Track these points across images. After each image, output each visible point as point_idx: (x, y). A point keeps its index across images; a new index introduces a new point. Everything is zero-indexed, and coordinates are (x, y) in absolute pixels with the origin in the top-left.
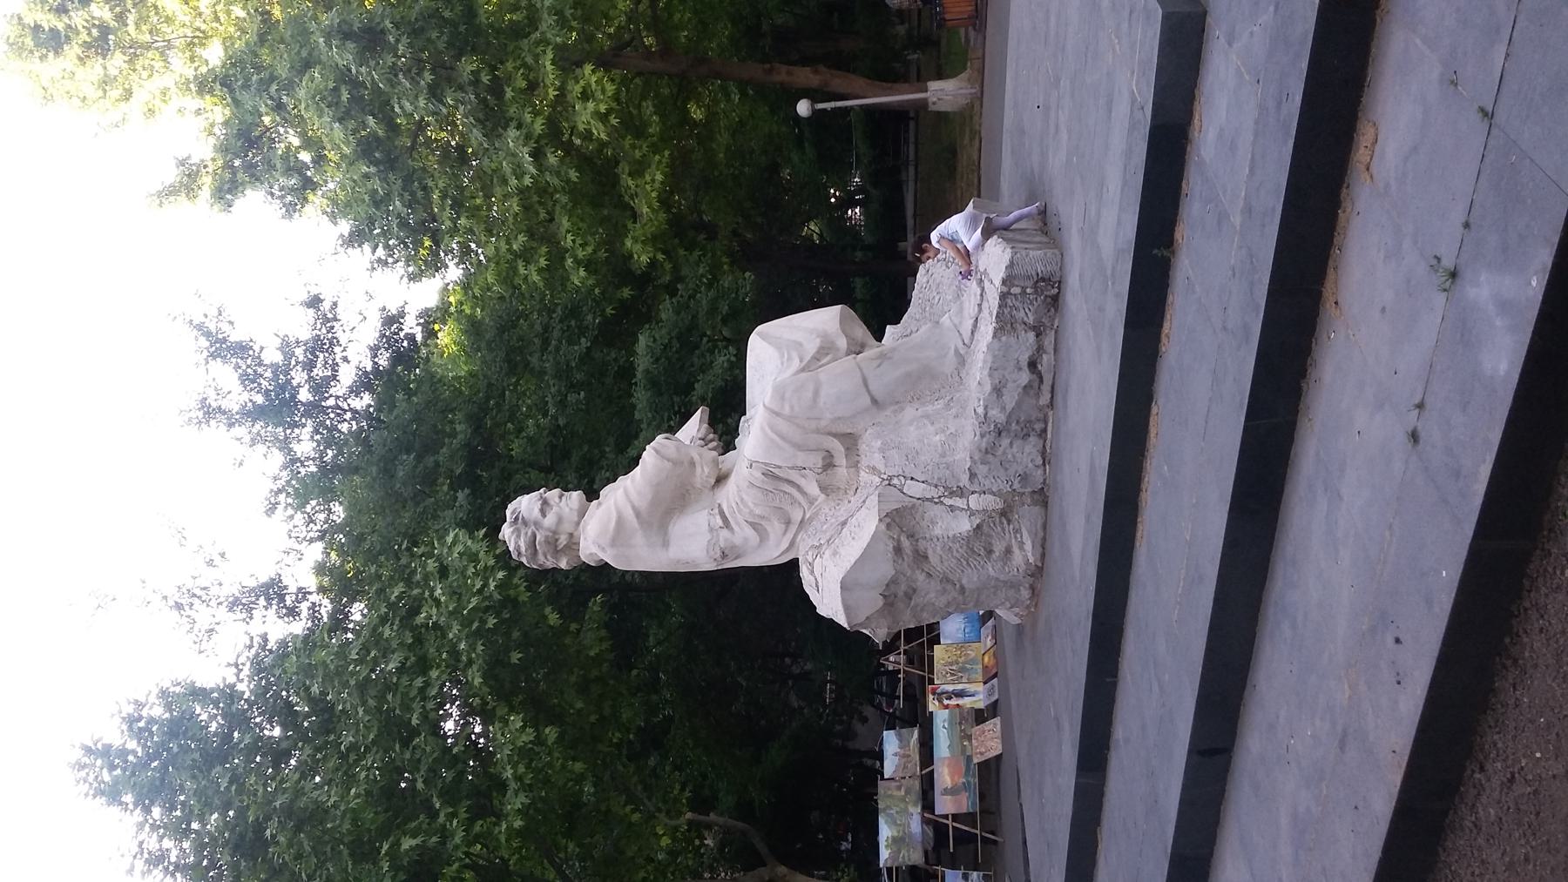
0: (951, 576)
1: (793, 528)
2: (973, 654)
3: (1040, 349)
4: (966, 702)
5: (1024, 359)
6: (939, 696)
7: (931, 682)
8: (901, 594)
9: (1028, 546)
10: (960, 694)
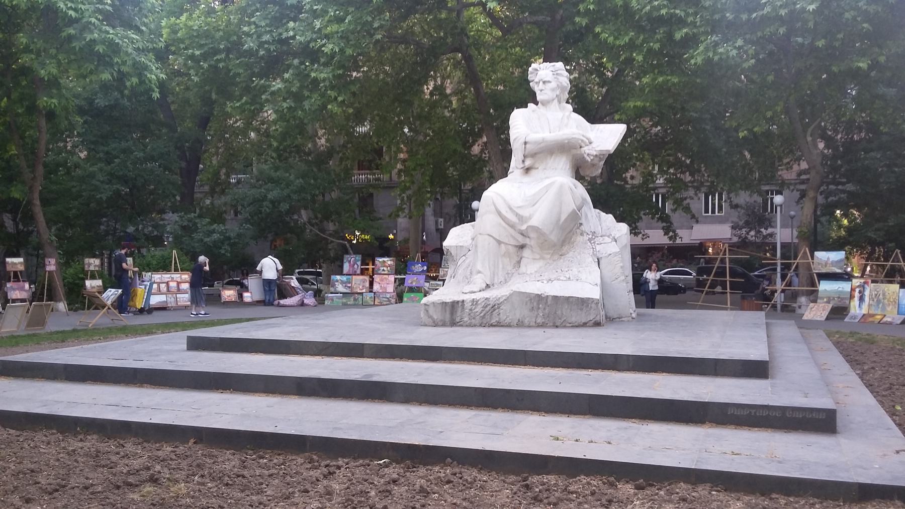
2: (889, 309)
4: (855, 302)
6: (862, 287)
7: (873, 282)
10: (861, 299)
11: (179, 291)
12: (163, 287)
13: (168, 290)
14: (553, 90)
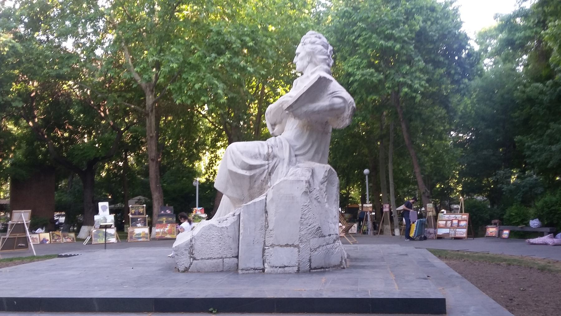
11: (458, 226)
12: (449, 223)
13: (451, 226)
14: (302, 59)
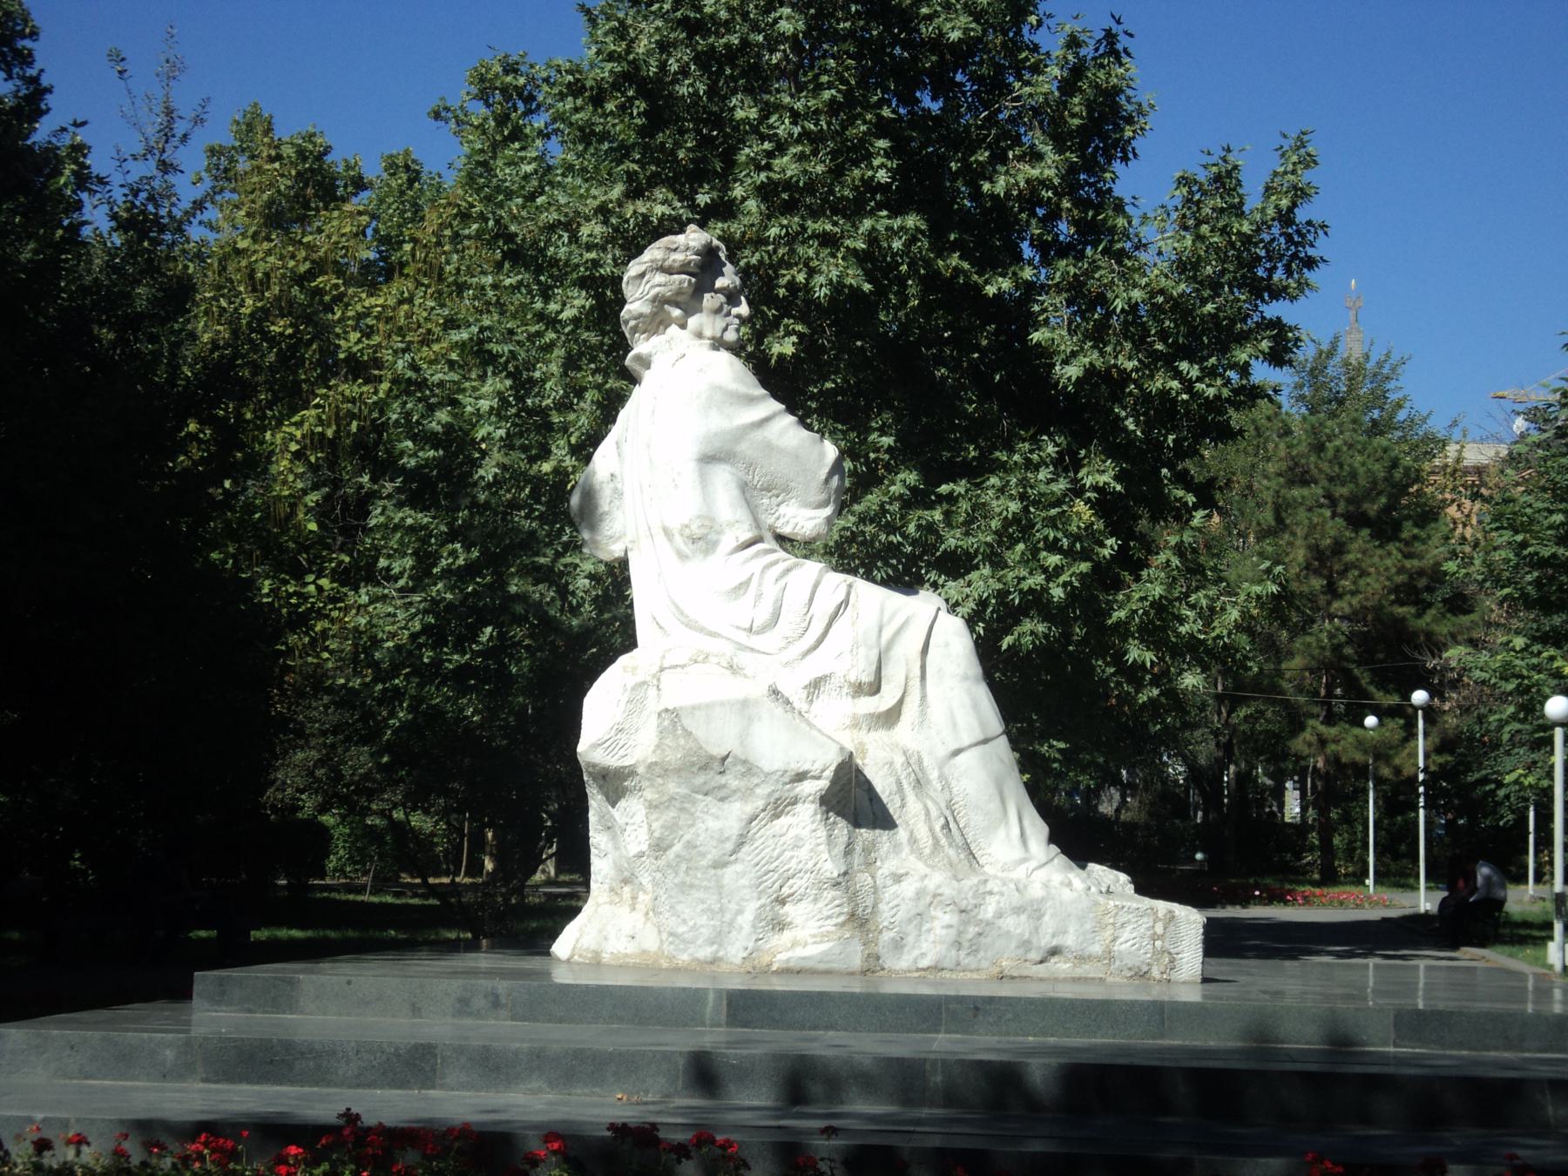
0: (746, 849)
1: (742, 637)
3: (1082, 958)
5: (1069, 941)
8: (723, 780)
9: (800, 952)
